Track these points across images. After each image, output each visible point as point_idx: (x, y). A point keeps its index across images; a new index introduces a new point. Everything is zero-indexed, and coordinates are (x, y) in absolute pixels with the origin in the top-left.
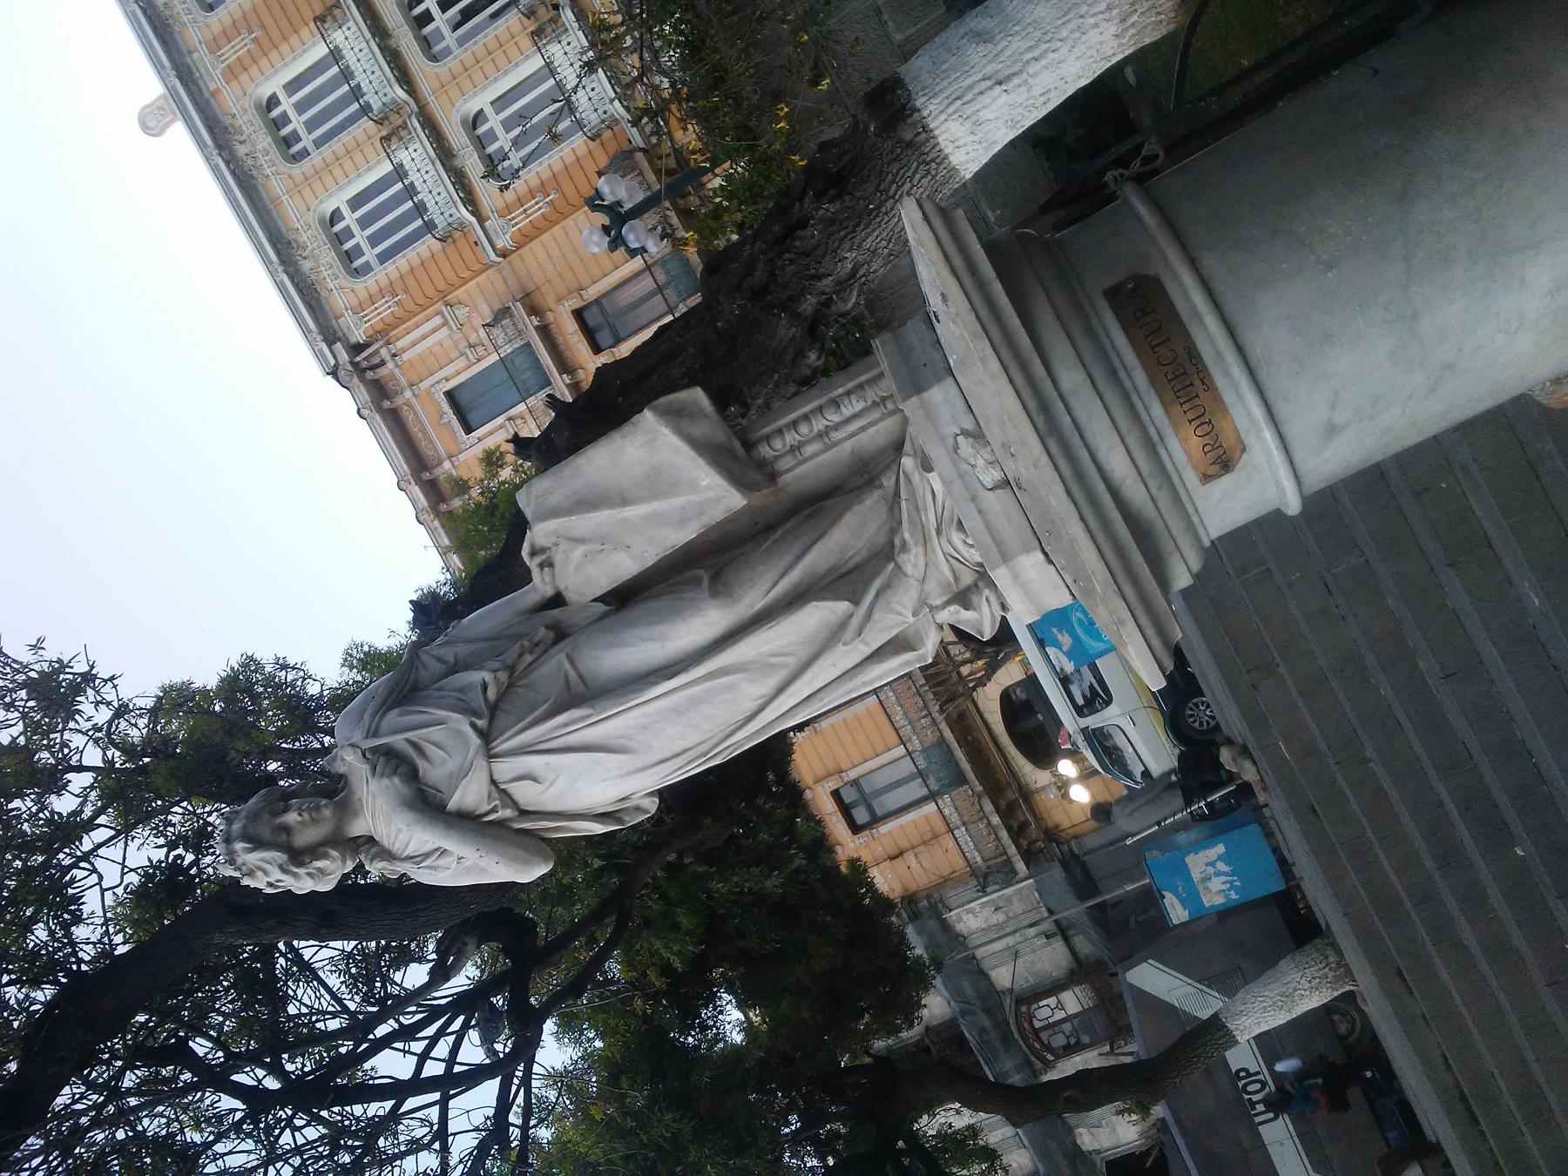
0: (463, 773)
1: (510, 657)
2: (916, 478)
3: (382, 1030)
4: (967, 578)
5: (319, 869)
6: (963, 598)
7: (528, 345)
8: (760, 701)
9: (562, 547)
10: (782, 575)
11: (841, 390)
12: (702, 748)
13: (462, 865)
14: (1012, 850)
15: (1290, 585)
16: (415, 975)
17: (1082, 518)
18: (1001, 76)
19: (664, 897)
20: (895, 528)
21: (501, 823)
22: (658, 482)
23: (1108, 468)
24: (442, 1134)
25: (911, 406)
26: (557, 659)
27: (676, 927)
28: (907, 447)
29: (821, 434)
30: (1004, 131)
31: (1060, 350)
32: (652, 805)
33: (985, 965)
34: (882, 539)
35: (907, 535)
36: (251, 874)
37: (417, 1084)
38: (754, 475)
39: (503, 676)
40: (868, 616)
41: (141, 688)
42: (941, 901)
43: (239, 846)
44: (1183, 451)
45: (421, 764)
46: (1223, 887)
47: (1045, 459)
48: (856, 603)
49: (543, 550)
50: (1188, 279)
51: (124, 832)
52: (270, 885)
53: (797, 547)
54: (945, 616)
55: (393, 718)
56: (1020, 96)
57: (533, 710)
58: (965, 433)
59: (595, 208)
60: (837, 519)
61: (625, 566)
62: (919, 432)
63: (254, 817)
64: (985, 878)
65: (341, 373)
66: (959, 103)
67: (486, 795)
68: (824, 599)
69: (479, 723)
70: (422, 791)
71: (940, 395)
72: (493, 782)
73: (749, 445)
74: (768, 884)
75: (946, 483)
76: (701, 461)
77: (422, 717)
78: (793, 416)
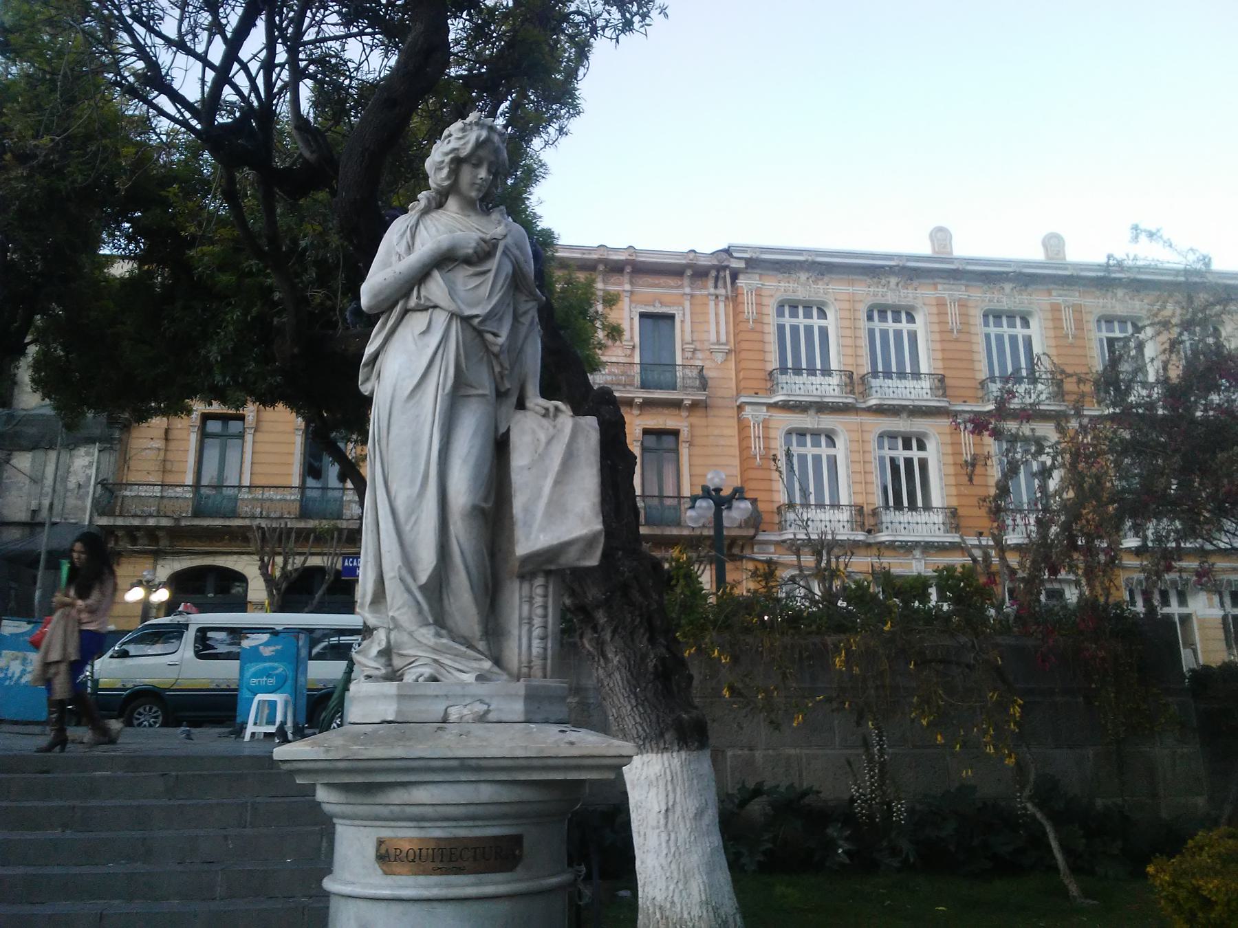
0: (452, 293)
1: (504, 358)
2: (475, 664)
3: (280, 48)
4: (397, 662)
5: (441, 169)
7: (674, 388)
9: (551, 429)
10: (462, 553)
11: (549, 645)
12: (384, 442)
14: (120, 522)
15: (226, 838)
16: (306, 89)
18: (670, 814)
19: (250, 274)
21: (407, 295)
22: (558, 508)
24: (180, 45)
25: (520, 687)
26: (487, 389)
27: (222, 268)
28: (496, 669)
31: (505, 794)
32: (365, 389)
33: (40, 454)
34: (450, 623)
35: (444, 641)
36: (463, 130)
37: (232, 55)
38: (529, 567)
39: (496, 349)
40: (409, 590)
41: (601, 47)
42: (111, 448)
43: (484, 134)
44: (406, 835)
45: (471, 270)
46: (10, 671)
47: (450, 755)
48: (422, 588)
49: (555, 416)
50: (502, 889)
52: (450, 135)
53: (474, 571)
55: (508, 268)
57: (466, 358)
61: (520, 459)
62: (501, 683)
63: (496, 151)
64: (112, 492)
65: (724, 256)
69: (476, 321)
71: (517, 708)
72: (435, 307)
73: (548, 573)
74: (215, 348)
75: (464, 685)
76: (555, 542)
77: (498, 287)
78: (550, 610)
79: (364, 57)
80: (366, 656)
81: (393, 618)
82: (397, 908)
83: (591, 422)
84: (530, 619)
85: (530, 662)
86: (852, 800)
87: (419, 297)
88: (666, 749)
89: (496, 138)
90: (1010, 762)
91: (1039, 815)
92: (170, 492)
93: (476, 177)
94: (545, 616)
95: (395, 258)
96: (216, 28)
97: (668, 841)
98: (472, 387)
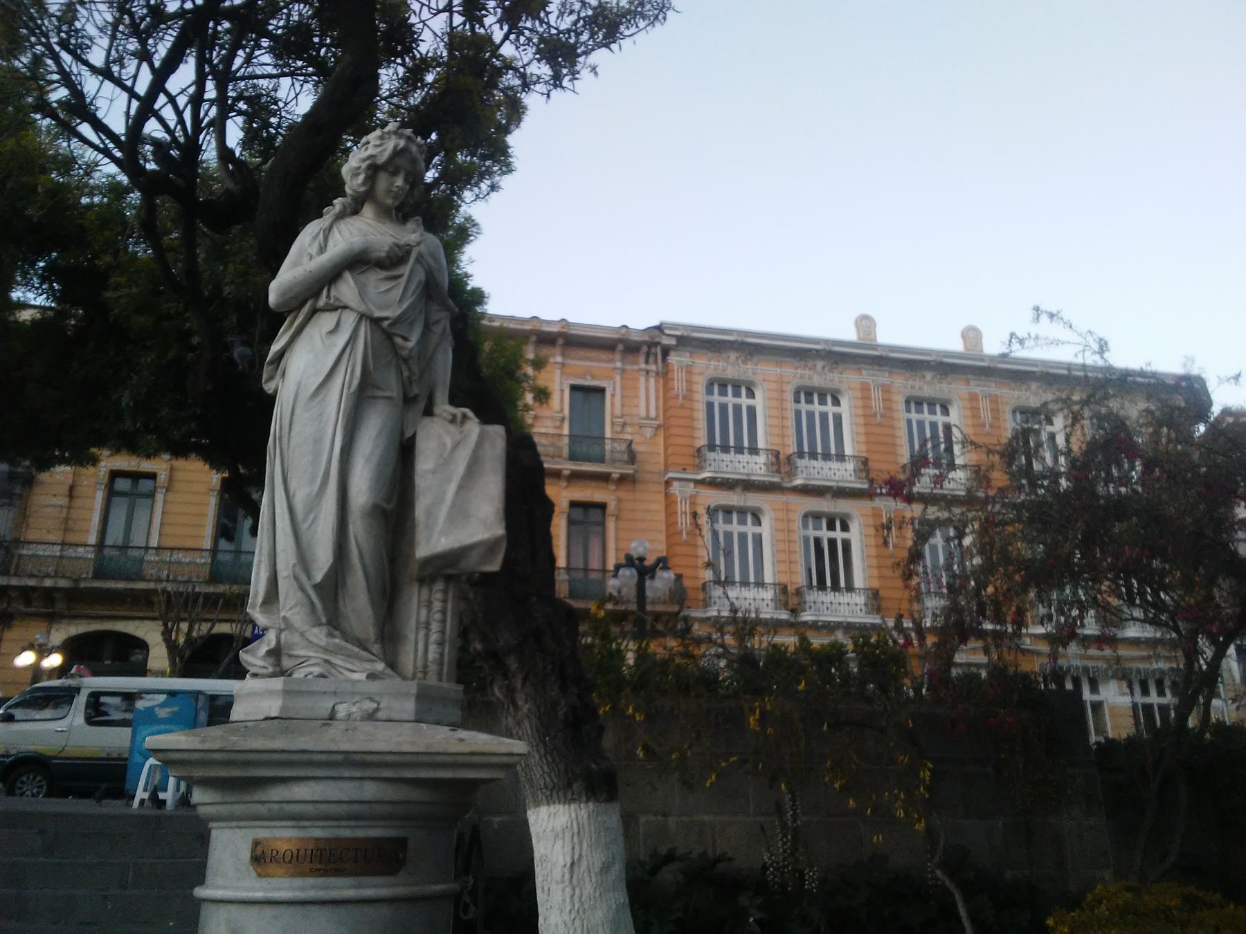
0: (362, 294)
2: (368, 666)
3: (210, 85)
4: (287, 663)
5: (358, 175)
6: (276, 653)
8: (291, 493)
11: (446, 651)
12: (285, 440)
13: (307, 253)
14: (14, 582)
16: (234, 133)
17: (283, 751)
18: (576, 868)
20: (346, 636)
21: (317, 295)
23: (303, 784)
25: (412, 687)
26: (394, 390)
28: (389, 671)
29: (428, 625)
30: (542, 851)
32: (269, 387)
35: (337, 641)
36: (381, 138)
37: (158, 86)
39: (405, 353)
40: (302, 589)
42: (10, 505)
43: (402, 143)
44: (284, 836)
45: (384, 274)
47: (333, 747)
48: (317, 587)
50: (384, 892)
51: (453, 39)
52: (368, 143)
55: (421, 275)
56: (557, 874)
57: (374, 355)
58: (377, 710)
59: (659, 560)
60: (373, 604)
61: (424, 463)
62: (394, 682)
63: (414, 161)
65: (656, 332)
66: (576, 831)
67: (342, 298)
68: (330, 569)
69: (386, 324)
72: (345, 307)
73: (448, 579)
76: (457, 545)
77: (410, 293)
78: (449, 614)
79: (292, 95)
80: (254, 655)
81: (284, 618)
82: (269, 911)
83: (497, 432)
84: (427, 625)
85: (426, 666)
86: (765, 868)
87: (328, 297)
88: (573, 800)
89: (414, 148)
90: (920, 826)
91: (948, 883)
92: (71, 552)
93: (392, 184)
94: (444, 621)
95: (306, 259)
96: (144, 56)
97: (572, 897)
98: (378, 388)
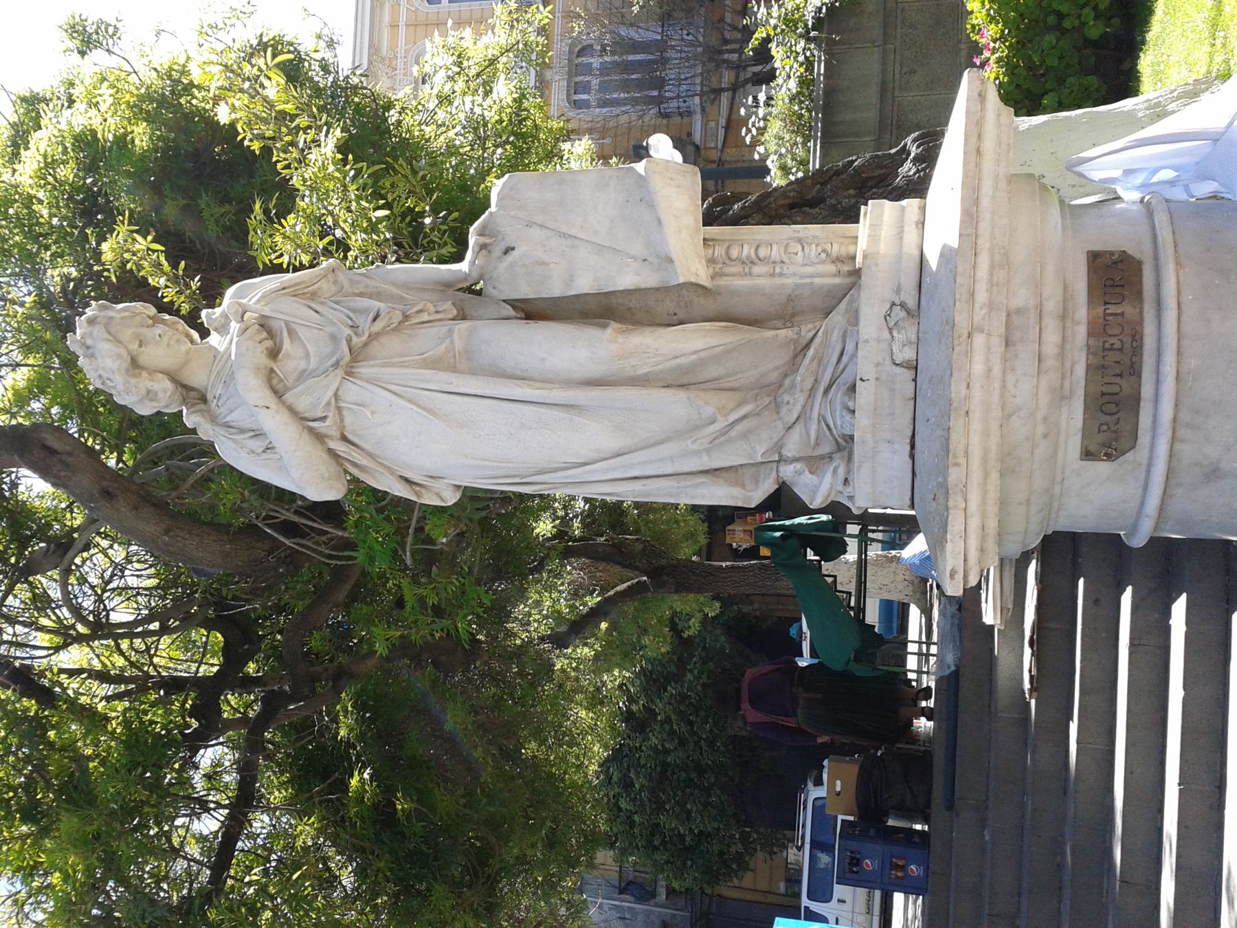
32: (451, 498)
34: (773, 377)
39: (398, 316)
54: (788, 472)
58: (903, 305)
70: (272, 371)
72: (336, 395)
